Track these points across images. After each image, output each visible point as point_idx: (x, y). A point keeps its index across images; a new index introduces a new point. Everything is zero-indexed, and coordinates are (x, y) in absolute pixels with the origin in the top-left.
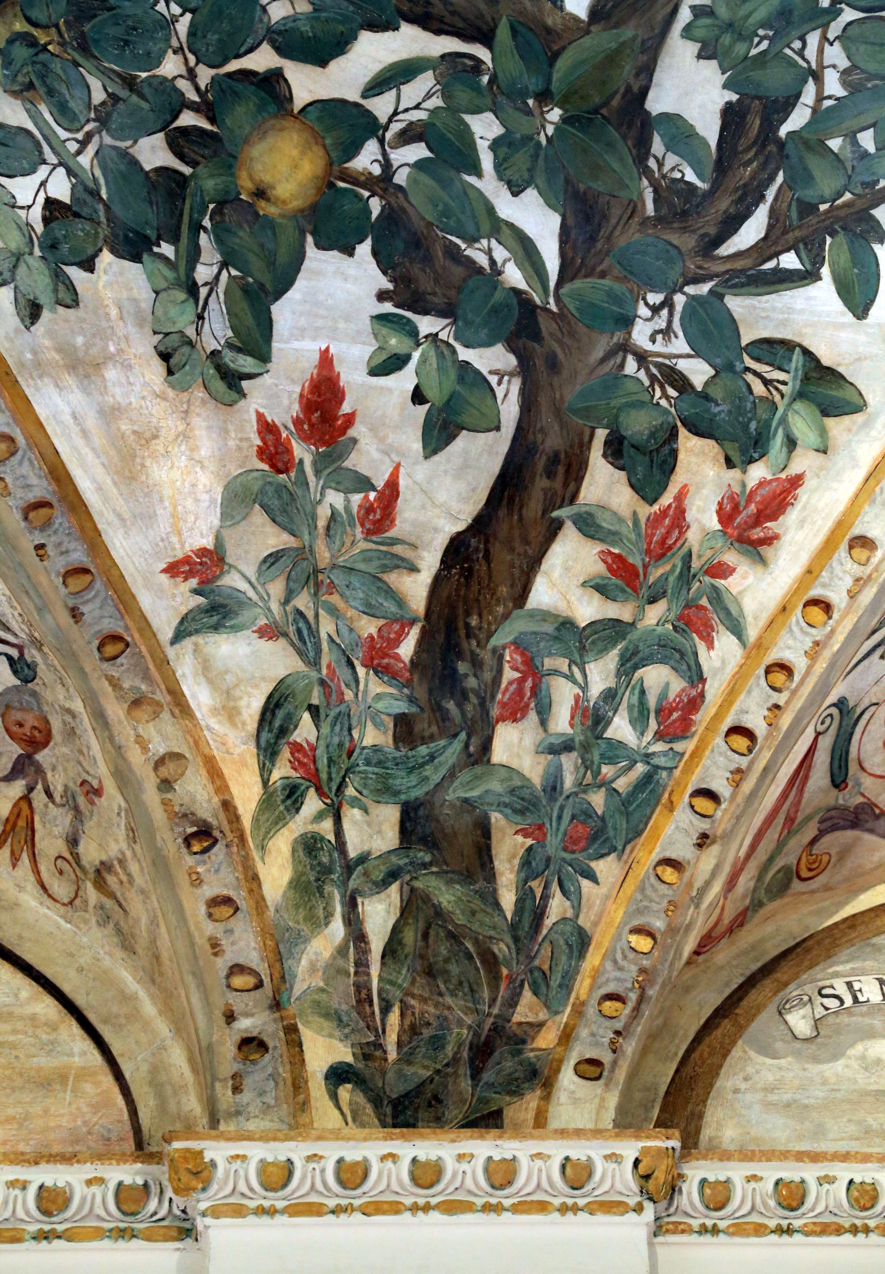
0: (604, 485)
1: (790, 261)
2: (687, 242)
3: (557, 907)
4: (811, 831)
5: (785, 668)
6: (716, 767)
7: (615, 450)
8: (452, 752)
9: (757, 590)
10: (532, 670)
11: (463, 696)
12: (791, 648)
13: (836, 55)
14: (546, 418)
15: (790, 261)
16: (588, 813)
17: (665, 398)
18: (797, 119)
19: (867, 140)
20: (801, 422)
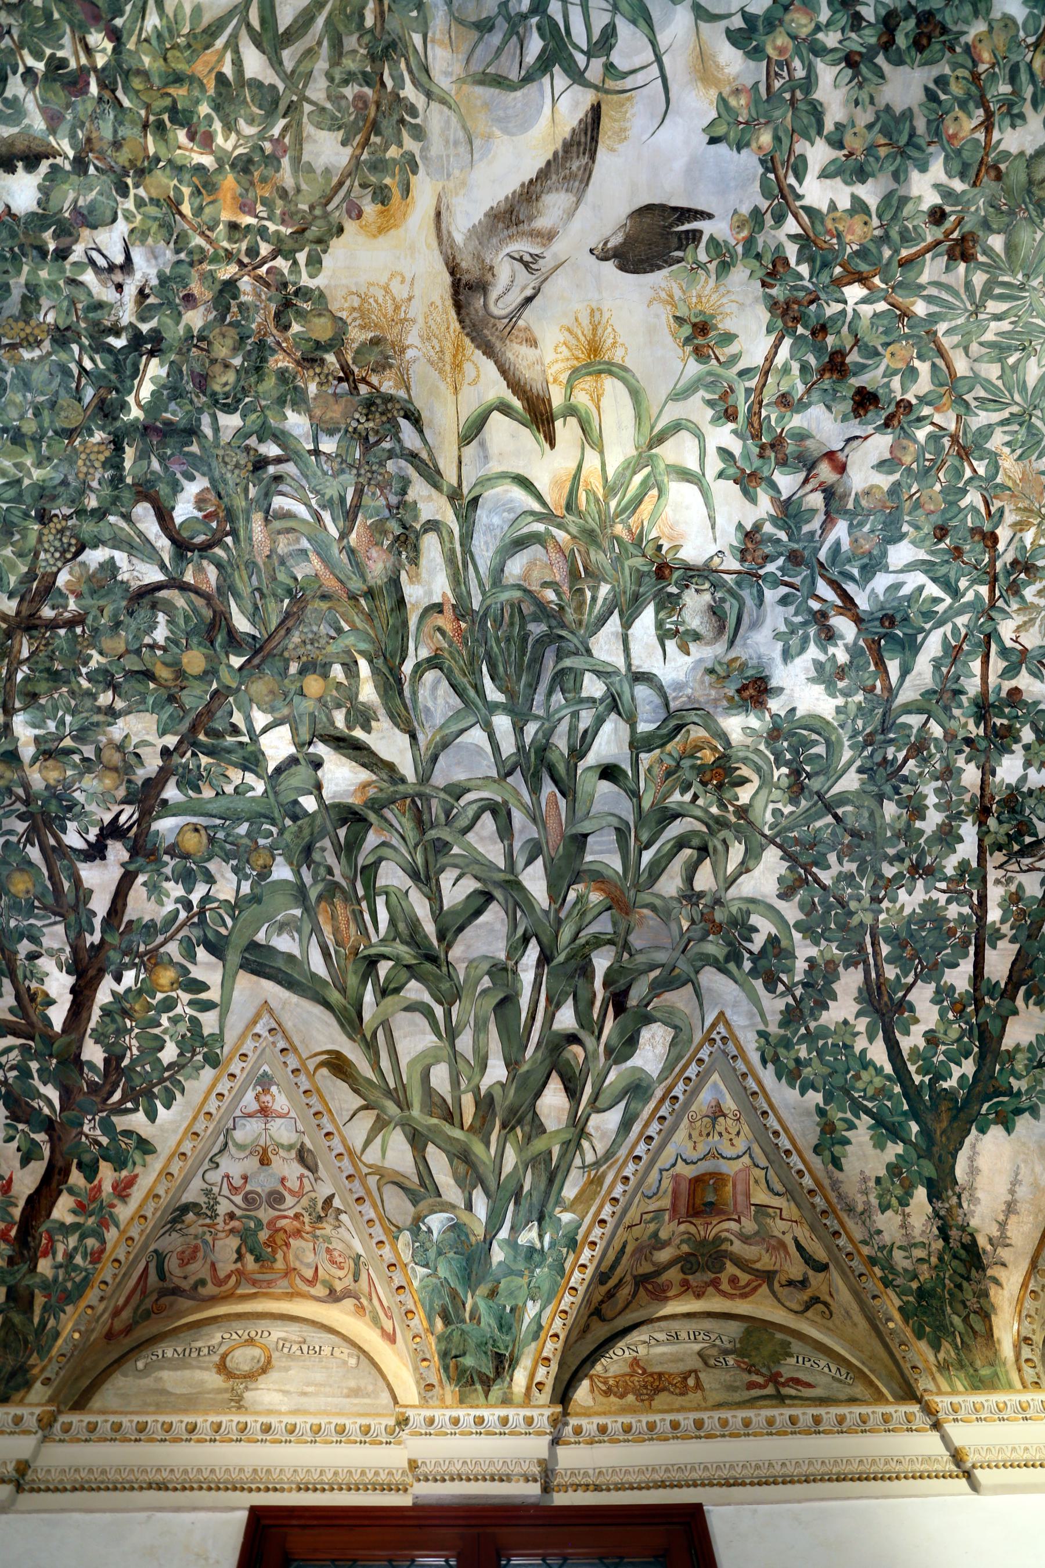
0: (76, 1178)
1: (129, 1105)
2: (98, 1100)
3: (52, 1322)
4: (155, 1296)
5: (131, 1239)
6: (107, 1271)
7: (80, 1166)
8: (25, 1268)
9: (124, 1212)
10: (51, 1240)
11: (29, 1249)
12: (134, 1232)
13: (134, 1042)
14: (58, 1156)
15: (129, 1105)
16: (65, 1289)
17: (95, 1149)
18: (126, 1062)
19: (148, 1068)
20: (137, 1156)
